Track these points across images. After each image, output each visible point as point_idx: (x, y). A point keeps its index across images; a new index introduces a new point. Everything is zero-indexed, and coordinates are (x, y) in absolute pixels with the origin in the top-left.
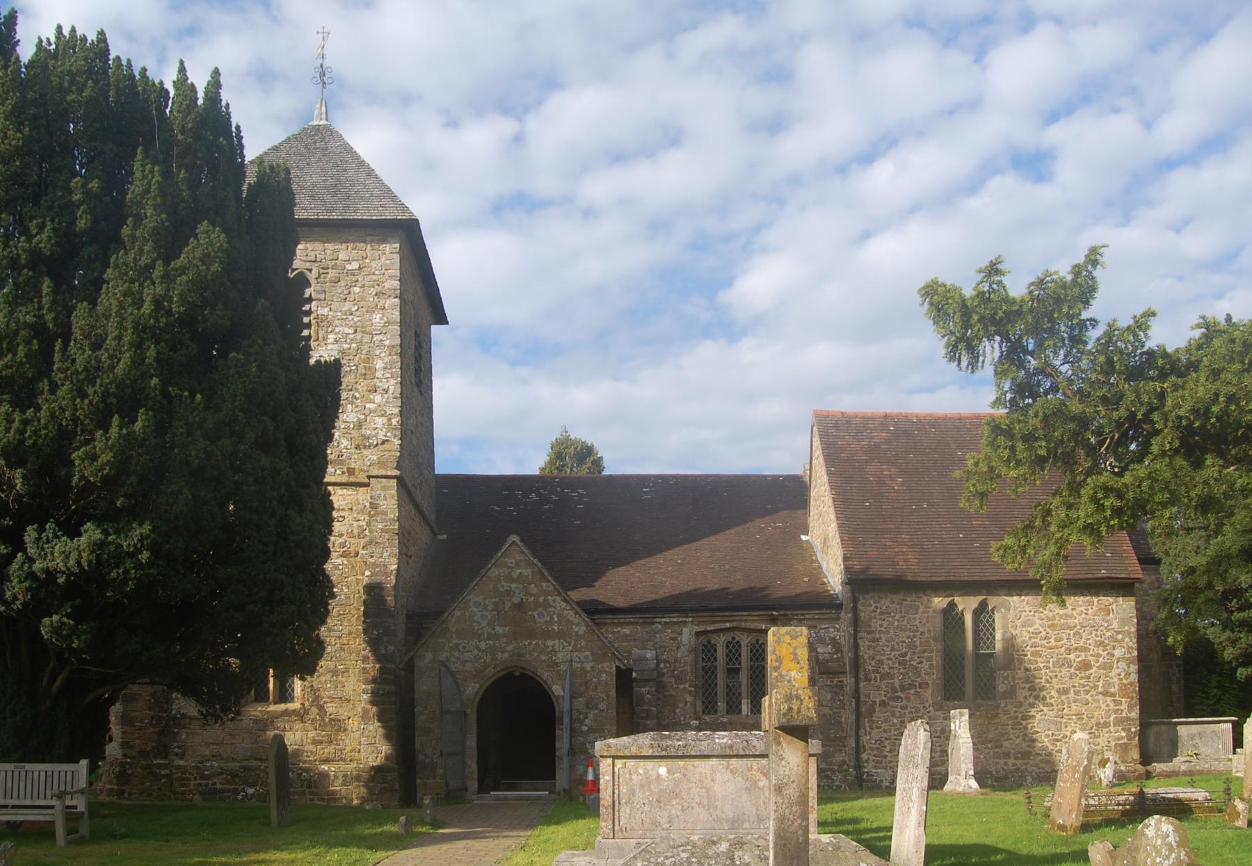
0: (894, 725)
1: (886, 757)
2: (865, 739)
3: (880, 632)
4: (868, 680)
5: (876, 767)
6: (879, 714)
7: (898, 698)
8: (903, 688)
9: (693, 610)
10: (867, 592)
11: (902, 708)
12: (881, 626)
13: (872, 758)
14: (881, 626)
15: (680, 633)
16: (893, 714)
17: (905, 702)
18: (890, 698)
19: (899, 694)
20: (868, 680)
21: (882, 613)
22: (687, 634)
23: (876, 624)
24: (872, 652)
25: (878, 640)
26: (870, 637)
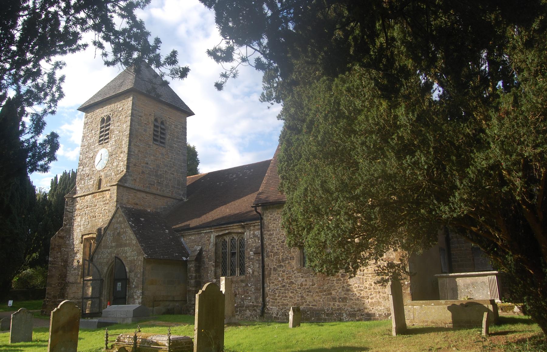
0: (279, 281)
2: (267, 289)
3: (273, 230)
4: (268, 256)
6: (273, 276)
7: (281, 266)
8: (283, 260)
9: (213, 226)
10: (267, 209)
11: (283, 272)
12: (274, 227)
14: (274, 227)
15: (210, 237)
16: (279, 275)
18: (278, 266)
19: (282, 264)
21: (274, 220)
22: (213, 237)
23: (271, 226)
24: (270, 241)
25: (272, 235)
26: (269, 233)
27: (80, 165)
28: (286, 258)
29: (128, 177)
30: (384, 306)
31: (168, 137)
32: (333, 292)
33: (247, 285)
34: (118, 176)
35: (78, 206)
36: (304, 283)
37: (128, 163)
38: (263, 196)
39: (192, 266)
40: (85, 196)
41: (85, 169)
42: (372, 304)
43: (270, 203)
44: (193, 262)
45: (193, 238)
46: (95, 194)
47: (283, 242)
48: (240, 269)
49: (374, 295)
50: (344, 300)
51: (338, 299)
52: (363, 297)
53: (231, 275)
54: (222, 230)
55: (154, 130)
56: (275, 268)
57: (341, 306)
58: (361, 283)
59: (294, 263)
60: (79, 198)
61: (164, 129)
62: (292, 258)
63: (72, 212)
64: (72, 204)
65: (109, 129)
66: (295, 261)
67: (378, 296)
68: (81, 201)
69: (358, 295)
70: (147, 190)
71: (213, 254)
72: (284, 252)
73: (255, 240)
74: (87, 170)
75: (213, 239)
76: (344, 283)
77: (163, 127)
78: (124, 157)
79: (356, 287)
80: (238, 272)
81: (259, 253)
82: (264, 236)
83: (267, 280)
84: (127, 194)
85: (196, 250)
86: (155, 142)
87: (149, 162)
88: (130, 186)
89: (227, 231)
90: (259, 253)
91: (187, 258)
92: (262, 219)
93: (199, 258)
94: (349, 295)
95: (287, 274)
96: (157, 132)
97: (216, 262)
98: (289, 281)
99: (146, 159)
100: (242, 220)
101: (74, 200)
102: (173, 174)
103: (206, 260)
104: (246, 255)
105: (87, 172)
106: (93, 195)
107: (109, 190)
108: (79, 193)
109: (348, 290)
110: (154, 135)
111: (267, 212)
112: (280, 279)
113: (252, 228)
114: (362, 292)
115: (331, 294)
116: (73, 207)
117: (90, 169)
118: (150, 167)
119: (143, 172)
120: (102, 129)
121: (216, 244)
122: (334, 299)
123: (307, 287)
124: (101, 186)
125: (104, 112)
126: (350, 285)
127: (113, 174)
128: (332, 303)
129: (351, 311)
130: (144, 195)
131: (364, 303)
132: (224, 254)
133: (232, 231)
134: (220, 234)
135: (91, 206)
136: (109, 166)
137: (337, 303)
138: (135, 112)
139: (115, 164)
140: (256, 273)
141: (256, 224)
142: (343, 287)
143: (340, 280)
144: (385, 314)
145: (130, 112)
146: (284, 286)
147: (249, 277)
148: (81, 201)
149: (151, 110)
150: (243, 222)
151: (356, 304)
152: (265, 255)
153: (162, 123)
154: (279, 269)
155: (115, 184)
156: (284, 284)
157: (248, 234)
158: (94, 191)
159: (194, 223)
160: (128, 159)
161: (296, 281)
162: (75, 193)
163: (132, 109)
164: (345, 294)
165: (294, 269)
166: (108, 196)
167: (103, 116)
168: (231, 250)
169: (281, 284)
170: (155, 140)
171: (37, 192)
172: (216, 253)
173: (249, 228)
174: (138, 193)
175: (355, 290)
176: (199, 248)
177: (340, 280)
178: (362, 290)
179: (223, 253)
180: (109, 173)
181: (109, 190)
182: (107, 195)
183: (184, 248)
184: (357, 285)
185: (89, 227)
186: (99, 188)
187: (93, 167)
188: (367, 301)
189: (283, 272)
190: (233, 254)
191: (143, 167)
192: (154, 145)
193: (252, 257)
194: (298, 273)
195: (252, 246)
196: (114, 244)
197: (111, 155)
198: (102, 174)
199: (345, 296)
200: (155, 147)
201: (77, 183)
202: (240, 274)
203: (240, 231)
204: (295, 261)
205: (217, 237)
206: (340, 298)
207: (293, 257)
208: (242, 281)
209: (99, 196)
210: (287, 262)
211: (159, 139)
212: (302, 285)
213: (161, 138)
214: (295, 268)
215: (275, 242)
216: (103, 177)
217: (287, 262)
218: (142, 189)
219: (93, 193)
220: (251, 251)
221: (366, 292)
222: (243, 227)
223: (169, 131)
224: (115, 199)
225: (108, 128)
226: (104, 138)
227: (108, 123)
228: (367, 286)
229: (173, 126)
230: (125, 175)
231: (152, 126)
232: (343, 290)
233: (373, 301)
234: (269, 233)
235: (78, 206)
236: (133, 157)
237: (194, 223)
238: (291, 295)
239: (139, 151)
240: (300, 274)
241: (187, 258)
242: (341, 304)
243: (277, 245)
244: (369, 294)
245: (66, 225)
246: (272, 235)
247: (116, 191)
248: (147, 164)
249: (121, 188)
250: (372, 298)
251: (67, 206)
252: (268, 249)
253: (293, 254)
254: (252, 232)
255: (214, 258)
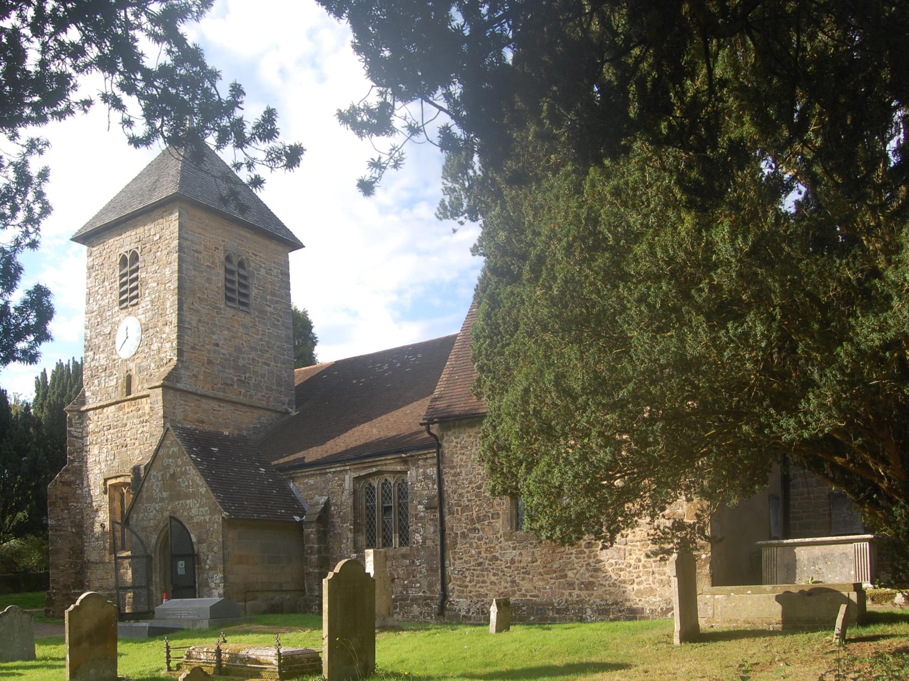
0: (472, 556)
1: (467, 587)
3: (461, 466)
4: (451, 513)
5: (459, 597)
6: (461, 546)
7: (475, 529)
8: (479, 520)
10: (449, 428)
11: (479, 539)
12: (461, 460)
13: (457, 588)
14: (461, 460)
15: (344, 480)
16: (471, 545)
17: (481, 533)
18: (470, 530)
19: (477, 525)
20: (451, 513)
21: (462, 448)
23: (457, 459)
24: (454, 487)
25: (459, 474)
26: (453, 471)
27: (87, 349)
28: (485, 516)
29: (183, 371)
30: (661, 596)
31: (254, 292)
32: (570, 574)
33: (413, 562)
34: (162, 370)
35: (91, 426)
36: (516, 559)
37: (179, 344)
38: (441, 405)
39: (311, 532)
40: (102, 407)
41: (97, 357)
42: (640, 593)
43: (454, 416)
44: (313, 525)
45: (311, 482)
46: (122, 404)
47: (479, 487)
48: (400, 536)
49: (643, 578)
50: (589, 586)
51: (579, 585)
52: (625, 582)
53: (384, 546)
54: (365, 468)
55: (226, 279)
56: (463, 533)
57: (583, 597)
58: (620, 558)
59: (499, 524)
60: (91, 412)
61: (245, 278)
62: (496, 516)
63: (82, 438)
64: (81, 423)
65: (136, 279)
66: (500, 521)
67: (651, 579)
68: (96, 418)
69: (614, 577)
70: (221, 395)
71: (349, 509)
72: (482, 505)
73: (427, 485)
74: (102, 359)
75: (348, 484)
76: (589, 557)
77: (242, 272)
78: (171, 332)
79: (612, 565)
80: (396, 540)
81: (436, 508)
82: (444, 477)
83: (450, 554)
84: (182, 402)
85: (317, 504)
86: (229, 304)
87: (221, 343)
88: (188, 387)
89: (374, 470)
90: (436, 508)
91: (301, 517)
92: (439, 446)
93: (325, 516)
94: (597, 577)
95: (486, 543)
96: (232, 282)
97: (355, 523)
98: (489, 556)
99: (215, 337)
100: (403, 448)
101: (83, 415)
102: (268, 365)
103: (337, 520)
104: (411, 511)
105: (103, 362)
106: (117, 406)
107: (148, 396)
108: (91, 403)
109: (596, 570)
110: (227, 288)
111: (450, 433)
112: (473, 552)
113: (421, 463)
114: (622, 573)
115: (566, 576)
116: (83, 429)
117: (108, 358)
118: (223, 351)
119: (210, 362)
120: (124, 279)
121: (355, 492)
122: (571, 585)
123: (522, 565)
124: (133, 389)
125: (124, 243)
126: (601, 561)
127: (153, 365)
128: (567, 592)
129: (601, 605)
130: (214, 404)
131: (624, 592)
132: (371, 509)
133: (384, 468)
134: (362, 474)
135: (116, 427)
136: (143, 351)
137: (576, 592)
138: (185, 243)
139: (155, 347)
140: (429, 543)
141: (429, 456)
142: (589, 564)
143: (582, 552)
144: (662, 609)
145: (176, 242)
146: (480, 564)
147: (417, 549)
148: (96, 418)
149: (219, 239)
150: (405, 452)
151: (611, 594)
152: (446, 510)
153: (241, 265)
154: (471, 535)
155: (157, 384)
156: (481, 560)
157: (414, 474)
158: (118, 399)
159: (312, 454)
160: (179, 337)
161: (503, 555)
162: (83, 403)
163: (180, 237)
164: (591, 576)
165: (499, 535)
166: (147, 408)
167: (122, 251)
168: (383, 503)
169: (476, 560)
170: (228, 299)
171: (11, 401)
172: (355, 507)
173: (414, 460)
174: (204, 401)
175: (610, 569)
176: (323, 500)
177: (582, 552)
178: (621, 570)
179: (367, 508)
180: (144, 364)
181: (148, 396)
182: (145, 405)
183: (295, 501)
184: (613, 561)
185: (115, 464)
186: (129, 392)
187: (112, 354)
188: (630, 587)
189: (479, 539)
190: (387, 510)
191: (209, 351)
192: (227, 309)
193: (422, 514)
194: (507, 540)
195: (421, 495)
196: (165, 494)
197: (145, 329)
198: (132, 365)
199: (591, 579)
200: (229, 313)
201: (85, 383)
202: (401, 544)
203: (399, 468)
204: (500, 521)
205: (355, 479)
206: (582, 583)
207: (498, 514)
208: (404, 556)
209: (129, 407)
210: (486, 523)
211: (236, 296)
212: (513, 561)
213: (240, 294)
214: (501, 532)
215: (464, 488)
216: (133, 372)
217: (486, 523)
218: (210, 393)
219: (117, 403)
220: (420, 503)
221: (630, 572)
222: (405, 461)
223: (255, 281)
224: (161, 413)
225: (134, 275)
226: (129, 296)
227: (134, 267)
228: (632, 562)
229: (263, 271)
230: (176, 368)
231: (222, 272)
232: (587, 569)
233: (642, 587)
234: (453, 471)
235: (91, 427)
236: (189, 331)
237: (312, 454)
238: (494, 579)
239: (199, 321)
240: (510, 543)
241: (301, 517)
242: (584, 594)
243: (468, 492)
244: (635, 575)
245: (73, 461)
246: (459, 474)
247: (160, 397)
248: (217, 345)
249: (171, 391)
250: (639, 583)
251: (71, 426)
252: (452, 499)
253: (498, 508)
254: (421, 470)
255: (351, 517)
